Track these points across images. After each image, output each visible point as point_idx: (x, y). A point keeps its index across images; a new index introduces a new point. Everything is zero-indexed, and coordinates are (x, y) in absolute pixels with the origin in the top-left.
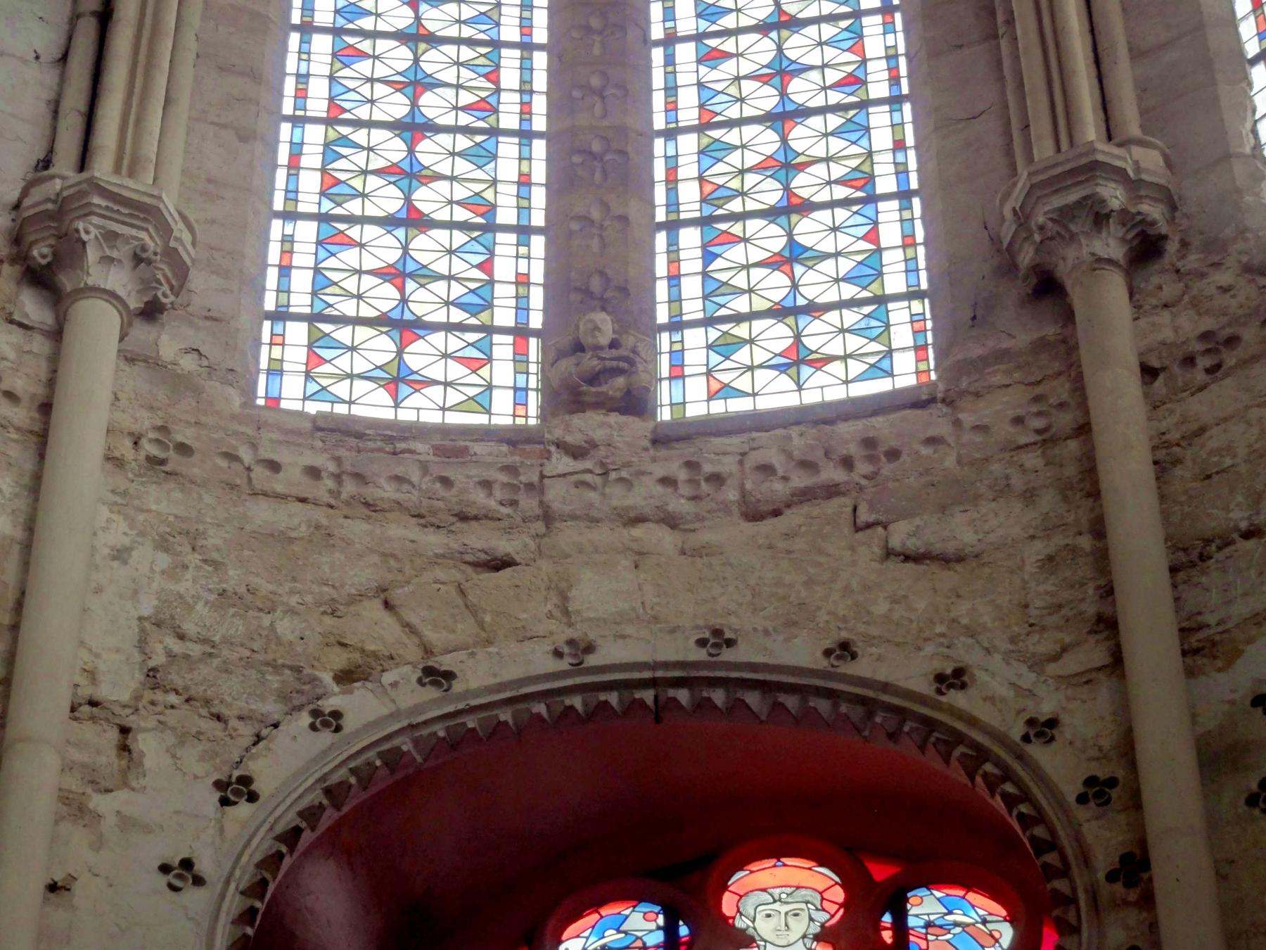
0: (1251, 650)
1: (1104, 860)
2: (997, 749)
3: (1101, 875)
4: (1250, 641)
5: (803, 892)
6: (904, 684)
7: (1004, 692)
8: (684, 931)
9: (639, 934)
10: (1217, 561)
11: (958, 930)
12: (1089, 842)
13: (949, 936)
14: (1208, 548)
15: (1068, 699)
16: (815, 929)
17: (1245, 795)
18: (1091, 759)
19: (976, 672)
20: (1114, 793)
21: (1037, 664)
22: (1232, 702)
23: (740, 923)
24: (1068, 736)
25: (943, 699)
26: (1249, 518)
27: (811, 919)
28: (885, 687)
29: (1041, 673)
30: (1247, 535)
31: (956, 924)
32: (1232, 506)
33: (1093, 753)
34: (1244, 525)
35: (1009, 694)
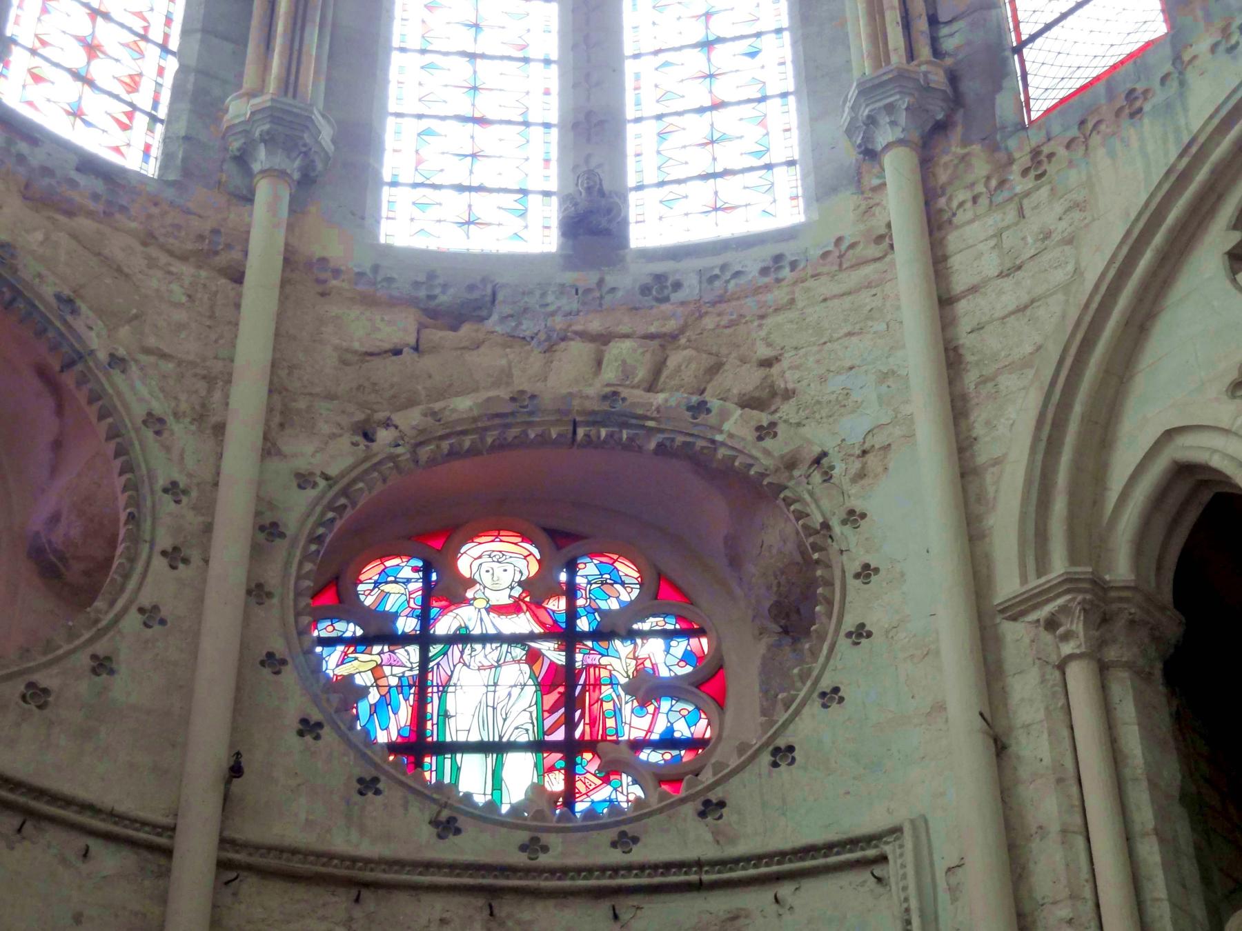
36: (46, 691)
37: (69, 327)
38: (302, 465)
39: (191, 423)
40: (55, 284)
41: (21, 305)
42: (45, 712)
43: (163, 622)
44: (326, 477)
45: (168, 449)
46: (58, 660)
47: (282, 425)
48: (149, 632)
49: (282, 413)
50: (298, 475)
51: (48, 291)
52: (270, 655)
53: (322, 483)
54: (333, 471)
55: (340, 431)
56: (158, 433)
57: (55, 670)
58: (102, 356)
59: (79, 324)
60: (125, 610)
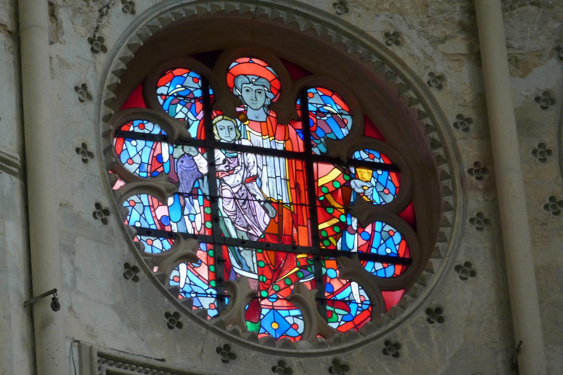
0: (536, 70)
1: (468, 162)
2: (416, 84)
3: (466, 170)
4: (536, 66)
5: (263, 80)
6: (371, 34)
7: (418, 53)
8: (211, 92)
9: (192, 89)
10: (518, 12)
11: (329, 115)
12: (460, 151)
13: (325, 118)
14: (514, 4)
15: (449, 67)
16: (268, 102)
17: (533, 149)
18: (460, 105)
19: (405, 38)
20: (472, 126)
21: (436, 42)
22: (527, 97)
23: (237, 92)
25: (390, 48)
27: (266, 97)
28: (362, 33)
29: (435, 48)
31: (329, 112)
35: (421, 55)
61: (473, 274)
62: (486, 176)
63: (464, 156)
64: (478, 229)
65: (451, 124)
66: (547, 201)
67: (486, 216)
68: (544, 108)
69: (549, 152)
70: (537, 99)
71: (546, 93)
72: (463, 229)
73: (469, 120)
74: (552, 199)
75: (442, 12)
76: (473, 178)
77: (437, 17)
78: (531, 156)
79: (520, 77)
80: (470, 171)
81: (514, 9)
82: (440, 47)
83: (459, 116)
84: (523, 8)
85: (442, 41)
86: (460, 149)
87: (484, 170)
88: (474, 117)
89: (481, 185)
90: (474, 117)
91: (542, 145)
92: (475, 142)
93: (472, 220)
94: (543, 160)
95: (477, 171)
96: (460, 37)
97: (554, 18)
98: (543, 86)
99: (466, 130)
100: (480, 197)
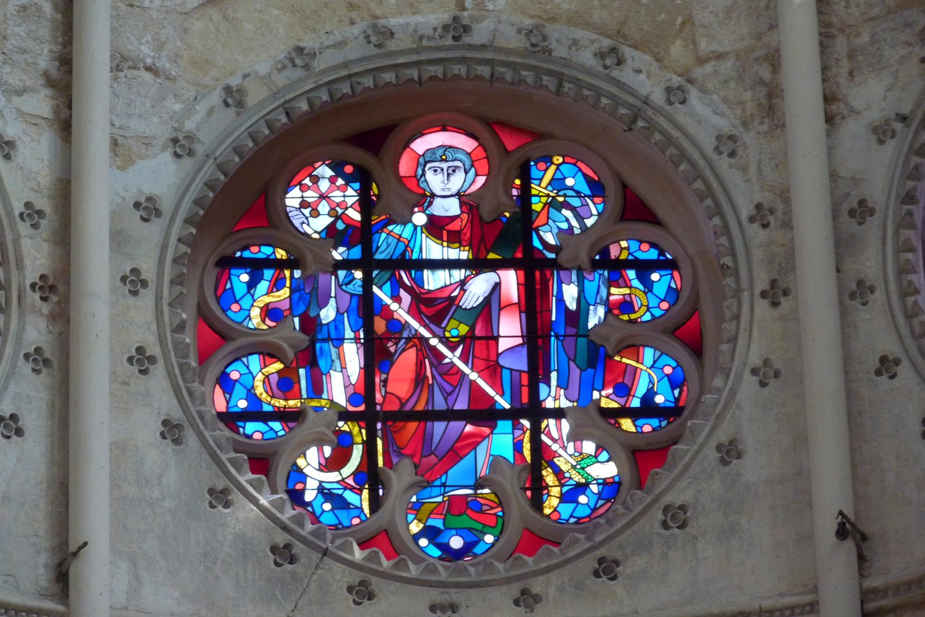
0: (140, 163)
3: (28, 282)
4: (141, 157)
10: (126, 76)
12: (24, 254)
14: (123, 64)
17: (122, 274)
18: (32, 189)
22: (124, 198)
24: (20, 160)
26: (154, 57)
30: (148, 69)
32: (143, 41)
33: (34, 184)
34: (149, 61)
36: (683, 508)
37: (618, 83)
38: (874, 115)
39: (761, 123)
40: (592, 42)
41: (567, 86)
42: (687, 530)
43: (777, 375)
44: (903, 119)
45: (744, 169)
46: (687, 467)
47: (851, 74)
48: (766, 391)
49: (850, 56)
50: (875, 130)
51: (587, 58)
52: (883, 360)
53: (898, 126)
54: (905, 109)
55: (910, 48)
56: (732, 154)
57: (685, 481)
58: (658, 97)
59: (625, 75)
60: (739, 377)
61: (19, 432)
62: (54, 298)
63: (28, 262)
64: (34, 370)
65: (17, 213)
66: (134, 353)
67: (48, 354)
68: (145, 220)
69: (144, 283)
70: (137, 205)
71: (149, 199)
72: (14, 365)
73: (40, 213)
74: (140, 350)
75: (25, 51)
76: (37, 296)
77: (16, 57)
78: (119, 283)
79: (119, 168)
80: (33, 286)
81: (122, 71)
82: (16, 99)
83: (28, 205)
84: (135, 72)
85: (20, 93)
86: (25, 252)
87: (52, 288)
88: (48, 210)
89: (45, 308)
90: (48, 210)
91: (134, 271)
92: (45, 245)
93: (27, 356)
94: (134, 293)
95: (41, 288)
96: (48, 92)
97: (175, 96)
98: (149, 189)
99: (35, 226)
100: (42, 324)
